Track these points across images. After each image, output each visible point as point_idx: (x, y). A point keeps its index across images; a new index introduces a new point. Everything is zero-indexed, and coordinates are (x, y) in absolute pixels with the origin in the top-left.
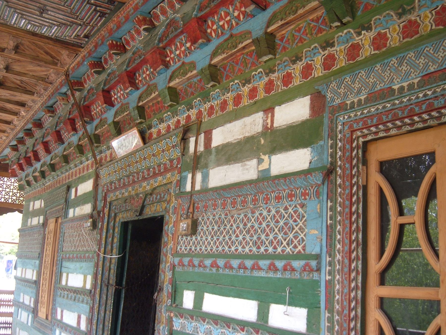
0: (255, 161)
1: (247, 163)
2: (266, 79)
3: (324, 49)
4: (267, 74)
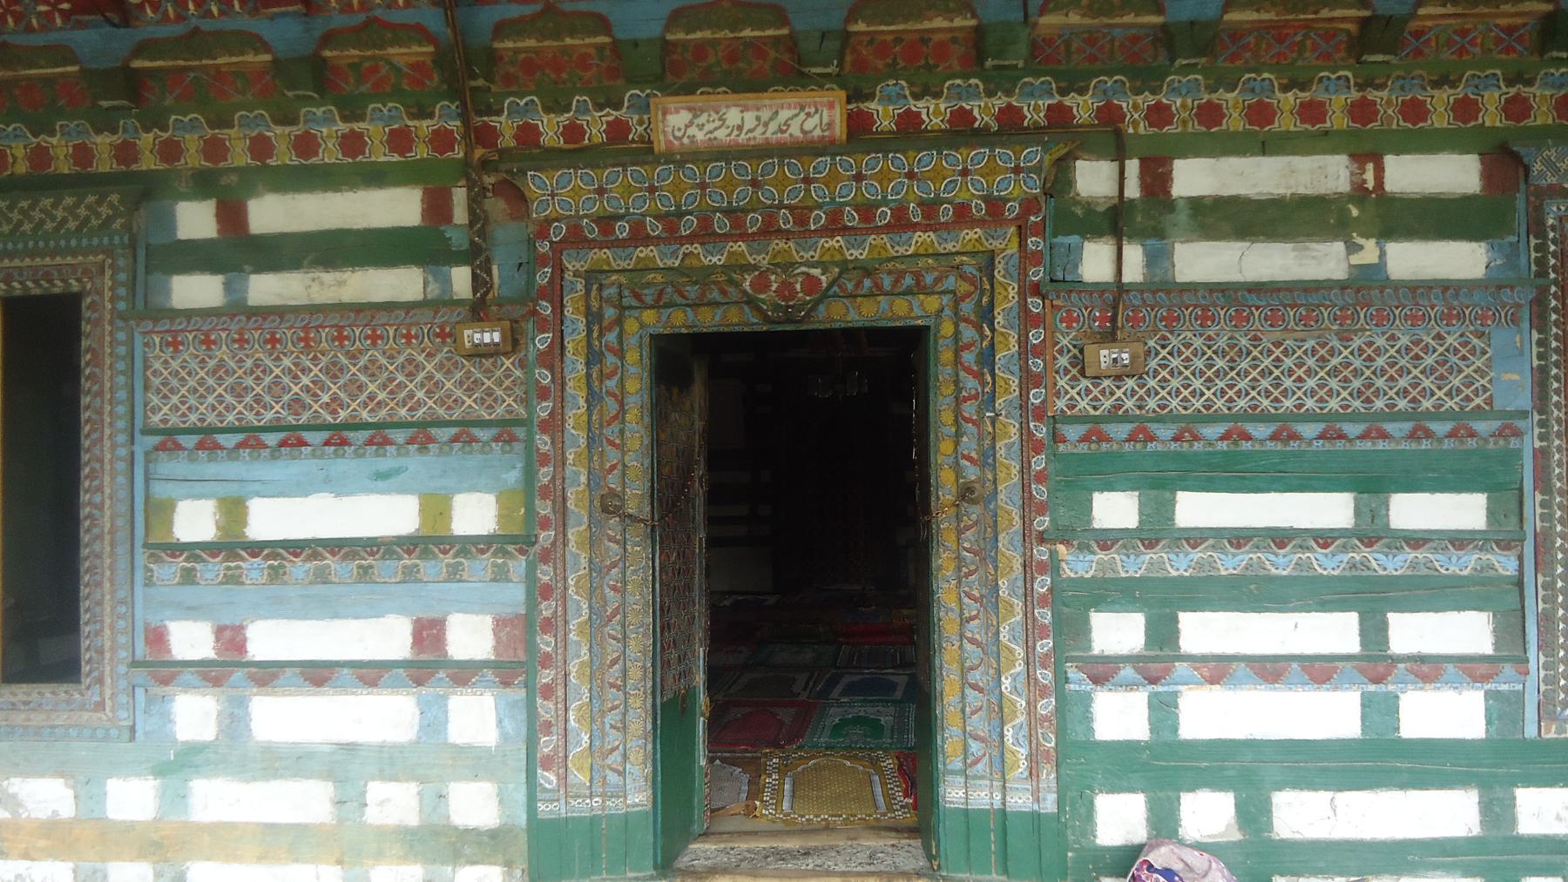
0: (1339, 246)
1: (1314, 245)
2: (1355, 95)
3: (1510, 83)
4: (1361, 87)
